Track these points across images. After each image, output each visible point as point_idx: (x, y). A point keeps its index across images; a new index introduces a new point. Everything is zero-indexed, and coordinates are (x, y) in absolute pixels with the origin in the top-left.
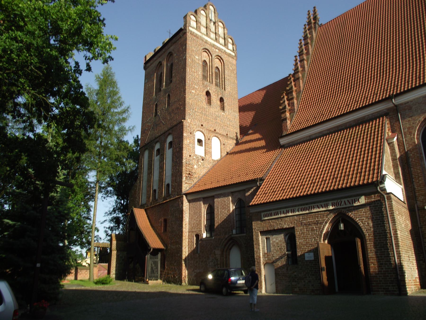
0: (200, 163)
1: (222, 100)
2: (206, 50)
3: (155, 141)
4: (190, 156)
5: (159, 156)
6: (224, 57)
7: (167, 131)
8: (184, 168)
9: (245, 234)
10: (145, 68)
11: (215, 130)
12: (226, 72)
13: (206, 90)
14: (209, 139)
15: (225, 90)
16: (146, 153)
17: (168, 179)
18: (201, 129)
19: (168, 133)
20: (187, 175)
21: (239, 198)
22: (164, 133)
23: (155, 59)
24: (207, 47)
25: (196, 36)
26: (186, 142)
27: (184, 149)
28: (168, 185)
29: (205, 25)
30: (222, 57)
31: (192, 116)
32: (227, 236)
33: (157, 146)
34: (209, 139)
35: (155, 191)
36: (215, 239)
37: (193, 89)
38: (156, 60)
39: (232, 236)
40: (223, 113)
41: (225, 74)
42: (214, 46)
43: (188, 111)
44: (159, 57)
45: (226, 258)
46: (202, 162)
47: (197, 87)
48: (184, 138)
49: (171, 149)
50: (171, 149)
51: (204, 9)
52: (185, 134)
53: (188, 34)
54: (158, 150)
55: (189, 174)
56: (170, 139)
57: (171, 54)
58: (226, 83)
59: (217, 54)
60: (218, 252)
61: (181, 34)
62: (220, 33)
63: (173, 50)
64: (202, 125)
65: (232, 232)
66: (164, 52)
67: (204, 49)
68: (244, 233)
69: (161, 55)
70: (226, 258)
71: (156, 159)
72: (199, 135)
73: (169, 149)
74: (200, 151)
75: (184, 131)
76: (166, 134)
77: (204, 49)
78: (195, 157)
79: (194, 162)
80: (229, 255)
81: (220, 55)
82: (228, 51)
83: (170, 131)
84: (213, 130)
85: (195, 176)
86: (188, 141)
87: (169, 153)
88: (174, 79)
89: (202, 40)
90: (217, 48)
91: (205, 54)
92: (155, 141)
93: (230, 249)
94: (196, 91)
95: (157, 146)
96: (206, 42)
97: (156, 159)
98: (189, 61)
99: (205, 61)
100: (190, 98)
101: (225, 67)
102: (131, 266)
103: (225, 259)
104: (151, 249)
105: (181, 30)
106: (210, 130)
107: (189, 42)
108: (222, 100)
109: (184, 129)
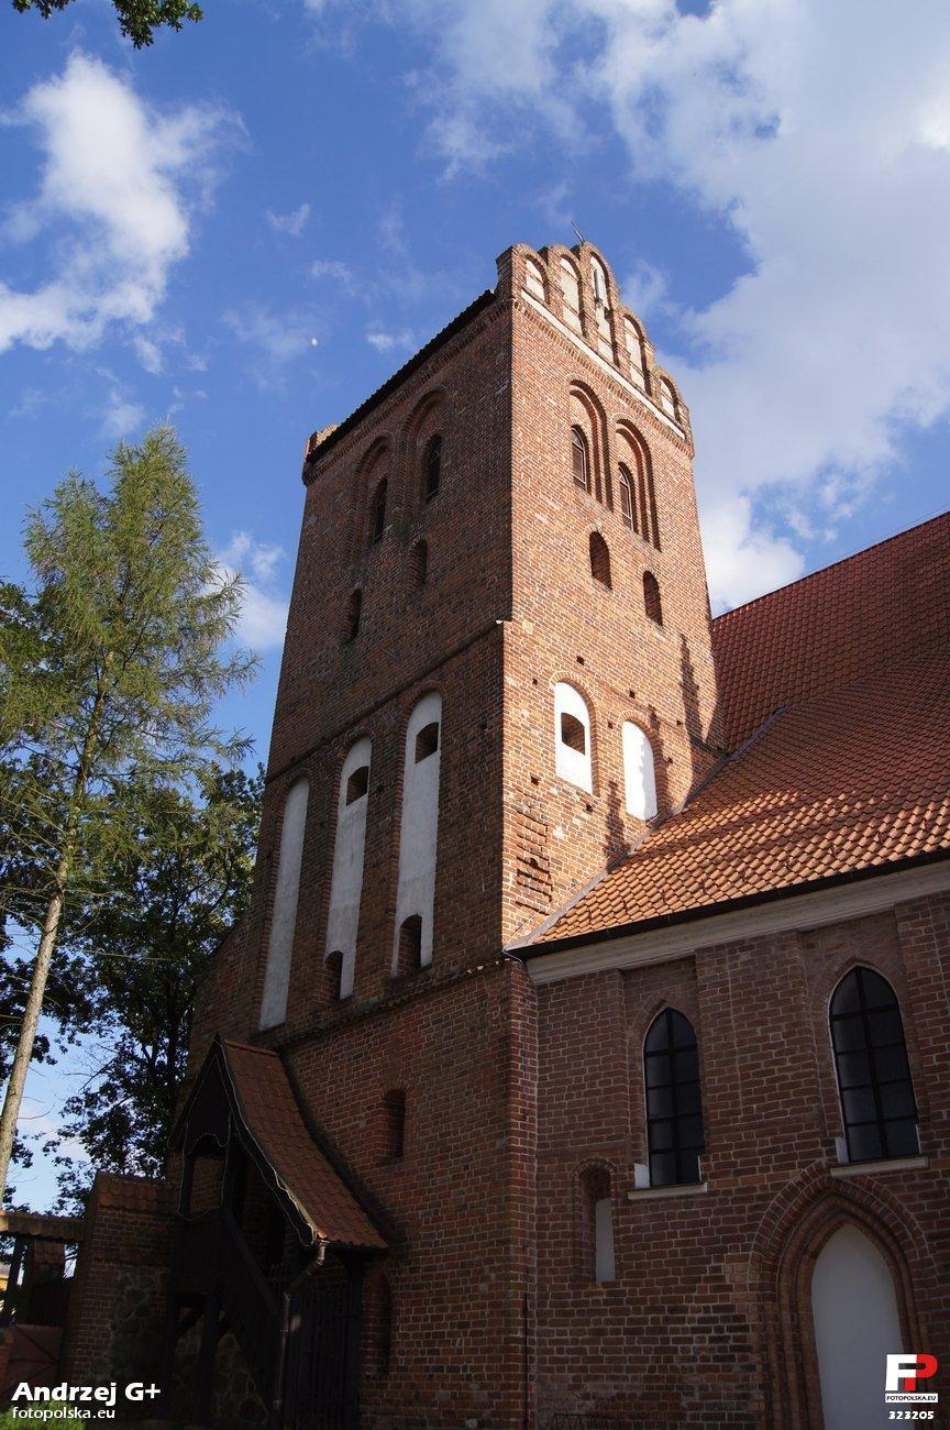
0: (576, 821)
1: (649, 580)
2: (584, 392)
3: (348, 735)
4: (535, 781)
5: (364, 799)
6: (648, 432)
7: (410, 685)
8: (508, 832)
9: (921, 1163)
10: (308, 477)
11: (632, 694)
12: (659, 486)
13: (591, 528)
14: (610, 726)
15: (657, 545)
16: (297, 806)
17: (416, 893)
18: (577, 677)
19: (416, 691)
20: (523, 867)
21: (853, 960)
22: (397, 694)
23: (356, 433)
24: (585, 380)
25: (545, 327)
26: (516, 713)
27: (507, 744)
28: (413, 924)
29: (576, 306)
30: (643, 430)
31: (538, 613)
32: (794, 1176)
33: (359, 758)
34: (610, 726)
35: (337, 958)
36: (711, 1193)
37: (541, 509)
38: (359, 437)
39: (835, 1173)
40: (657, 634)
41: (657, 492)
42: (611, 384)
43: (524, 591)
44: (378, 421)
45: (794, 1308)
46: (585, 816)
47: (557, 508)
48: (508, 694)
49: (434, 760)
50: (434, 760)
51: (573, 257)
52: (510, 680)
53: (518, 315)
54: (360, 782)
55: (533, 864)
56: (427, 714)
57: (430, 402)
58: (660, 524)
59: (625, 416)
60: (740, 1273)
61: (483, 316)
62: (629, 349)
63: (444, 383)
64: (580, 660)
65: (832, 1152)
66: (402, 400)
67: (575, 382)
68: (914, 1154)
69: (386, 415)
70: (794, 1308)
71: (351, 818)
72: (568, 702)
73: (419, 759)
74: (574, 767)
75: (507, 668)
76: (404, 698)
77: (575, 382)
78: (554, 791)
79: (553, 811)
80: (809, 1293)
81: (633, 420)
82: (658, 415)
83: (429, 681)
84: (624, 690)
85: (558, 876)
86: (526, 714)
87: (421, 781)
88: (448, 481)
89: (572, 351)
90: (622, 394)
91: (576, 403)
92: (348, 735)
93: (815, 1255)
94: (551, 520)
95: (359, 758)
96: (584, 362)
97: (351, 818)
98: (521, 403)
99: (577, 429)
100: (529, 537)
101: (654, 467)
102: (191, 1343)
103: (786, 1316)
104: (316, 1251)
105: (486, 300)
106: (613, 690)
107: (520, 341)
108: (649, 580)
109: (508, 657)
